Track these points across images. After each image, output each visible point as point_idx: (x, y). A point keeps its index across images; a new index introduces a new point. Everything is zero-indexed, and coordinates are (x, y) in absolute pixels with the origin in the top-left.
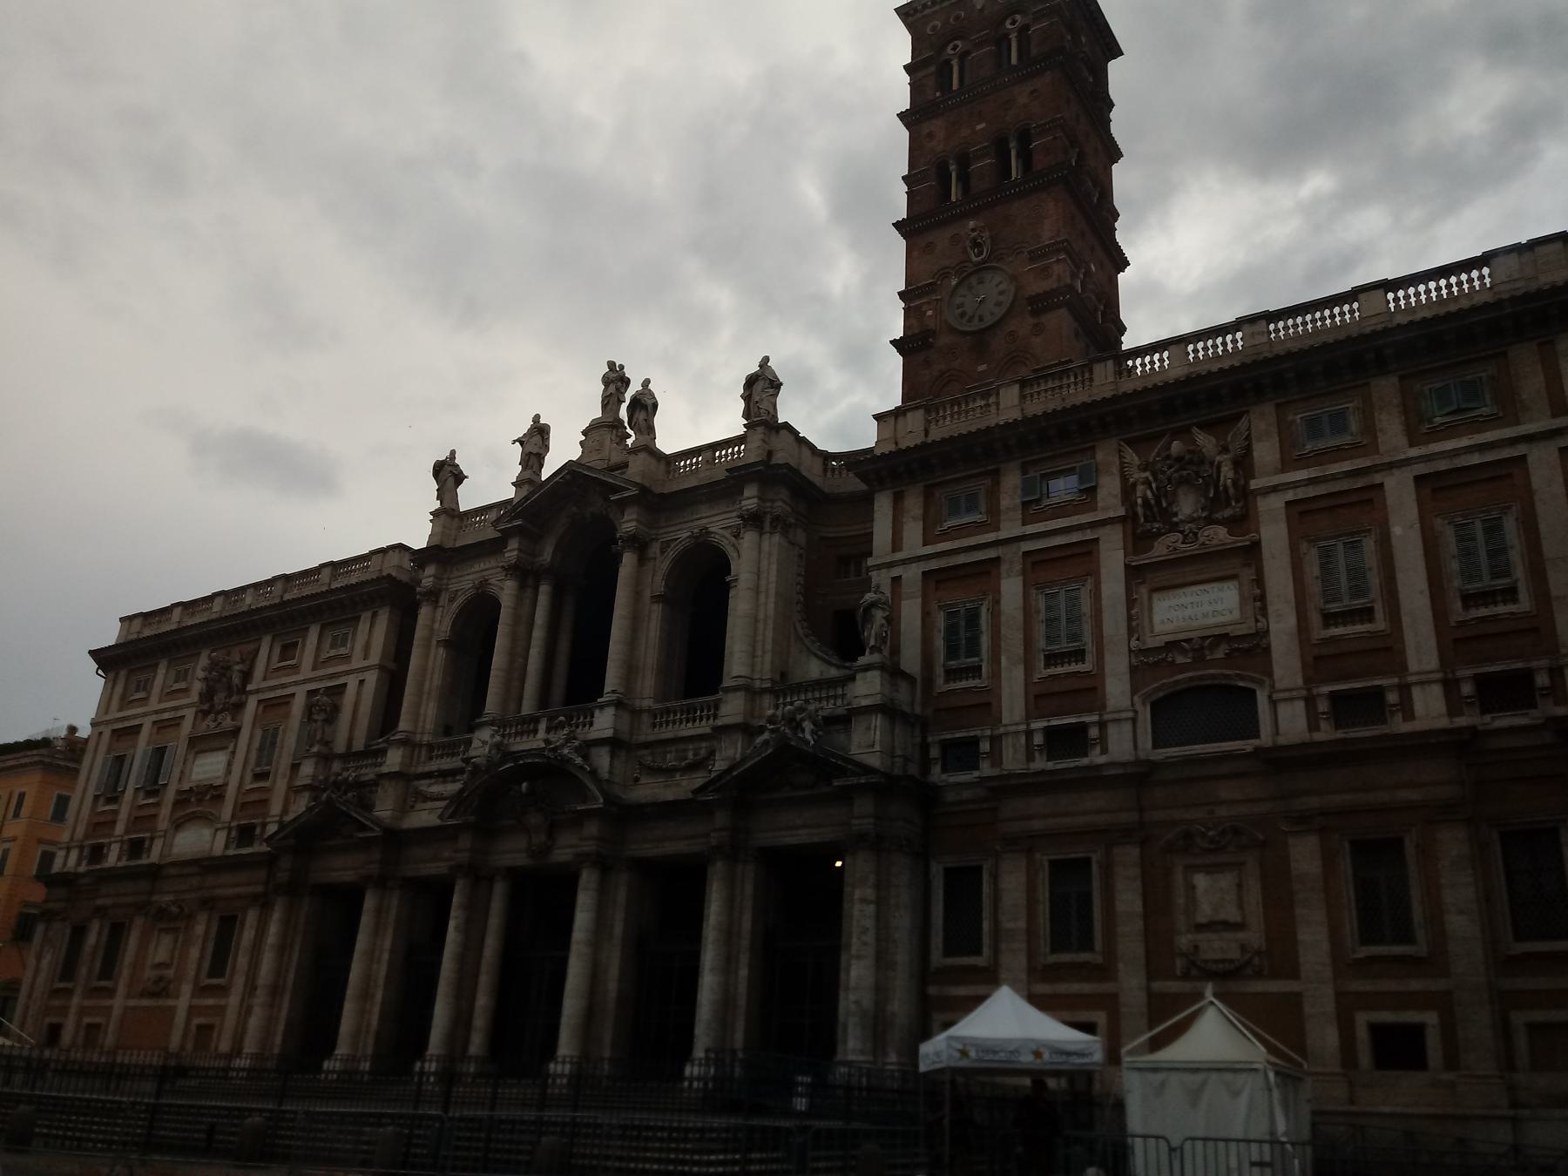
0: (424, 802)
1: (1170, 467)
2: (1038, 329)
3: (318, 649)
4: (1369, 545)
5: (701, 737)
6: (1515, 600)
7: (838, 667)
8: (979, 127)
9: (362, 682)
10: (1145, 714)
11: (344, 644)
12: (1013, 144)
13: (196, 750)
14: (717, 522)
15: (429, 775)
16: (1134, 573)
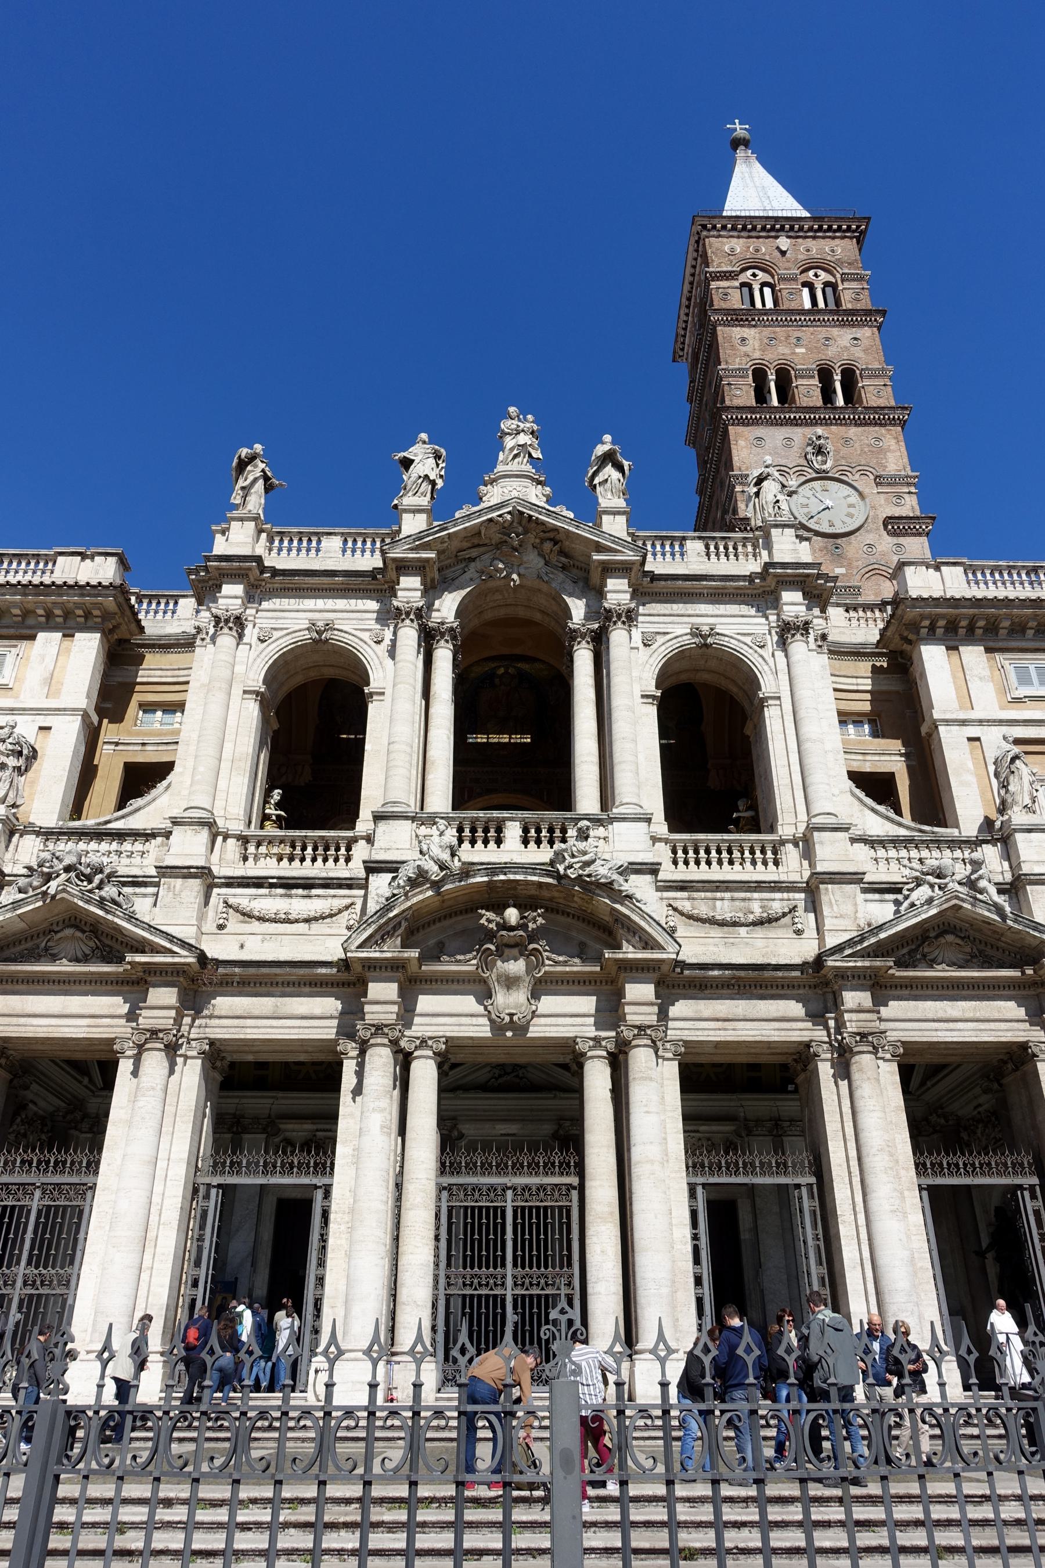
5: (776, 887)
12: (837, 378)
15: (258, 882)
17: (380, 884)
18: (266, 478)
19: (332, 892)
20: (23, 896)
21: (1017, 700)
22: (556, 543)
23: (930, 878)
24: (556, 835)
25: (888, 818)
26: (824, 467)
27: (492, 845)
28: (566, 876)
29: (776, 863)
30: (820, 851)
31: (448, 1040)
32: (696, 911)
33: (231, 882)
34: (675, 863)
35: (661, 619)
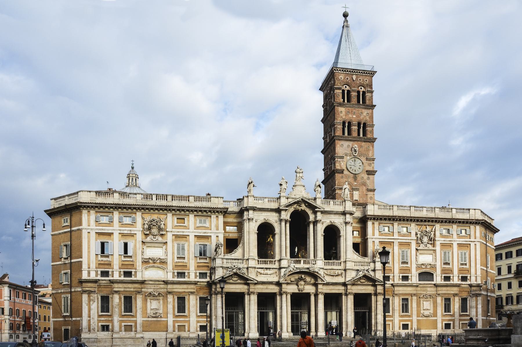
0: (260, 275)
1: (425, 232)
2: (368, 178)
3: (195, 223)
4: (451, 253)
5: (340, 270)
6: (466, 265)
7: (361, 257)
9: (217, 236)
11: (205, 222)
13: (146, 246)
14: (338, 221)
15: (262, 268)
16: (417, 250)
17: (283, 270)
18: (254, 185)
19: (273, 270)
20: (230, 272)
21: (382, 234)
22: (308, 204)
23: (362, 271)
24: (309, 263)
25: (358, 255)
26: (356, 155)
27: (299, 264)
28: (311, 271)
29: (340, 265)
30: (347, 265)
31: (293, 293)
32: (328, 274)
33: (258, 268)
34: (325, 265)
35: (325, 219)
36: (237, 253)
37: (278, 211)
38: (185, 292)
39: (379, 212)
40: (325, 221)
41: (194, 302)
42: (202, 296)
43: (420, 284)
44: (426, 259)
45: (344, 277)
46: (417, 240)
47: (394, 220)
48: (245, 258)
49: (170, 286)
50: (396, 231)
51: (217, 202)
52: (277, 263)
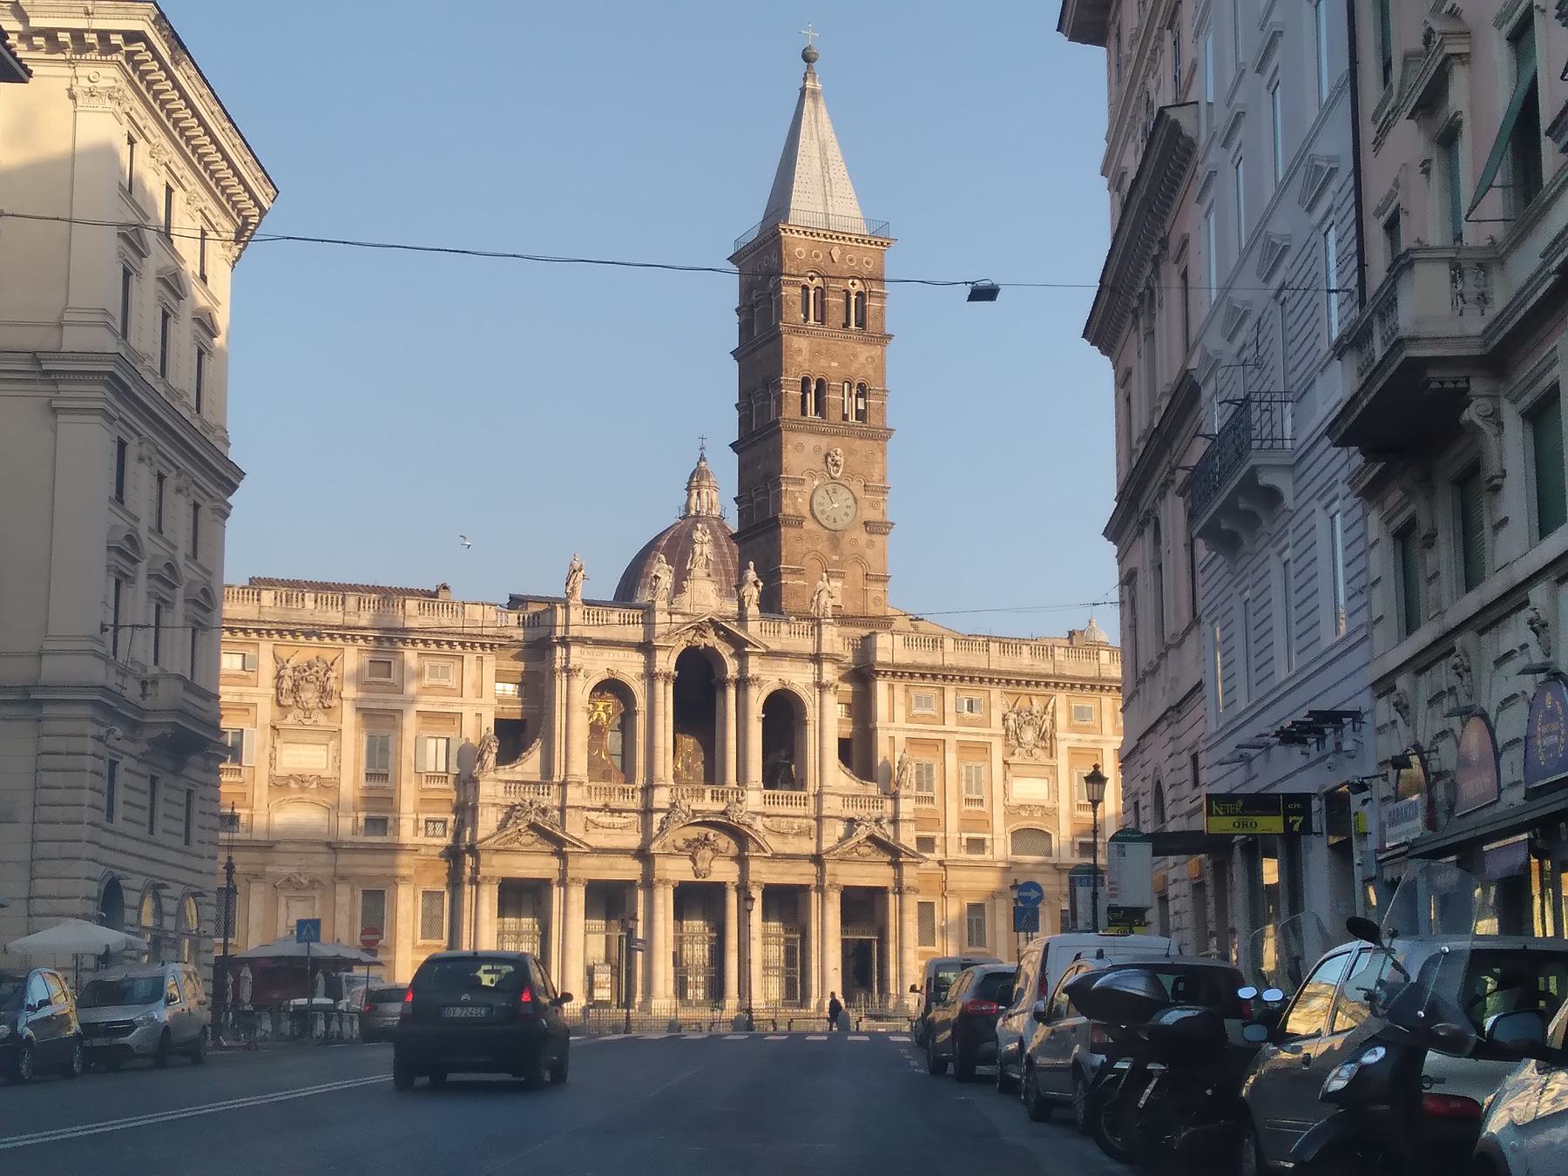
2: (871, 544)
8: (833, 364)
10: (1009, 836)
14: (799, 678)
16: (1005, 763)
19: (630, 814)
21: (914, 716)
29: (805, 805)
33: (589, 810)
36: (530, 765)
37: (647, 648)
38: (385, 875)
39: (904, 656)
40: (768, 677)
41: (410, 905)
42: (429, 887)
43: (1016, 863)
44: (1029, 789)
45: (815, 840)
46: (1007, 735)
47: (945, 678)
48: (556, 780)
49: (343, 859)
50: (950, 708)
51: (479, 618)
52: (638, 795)
